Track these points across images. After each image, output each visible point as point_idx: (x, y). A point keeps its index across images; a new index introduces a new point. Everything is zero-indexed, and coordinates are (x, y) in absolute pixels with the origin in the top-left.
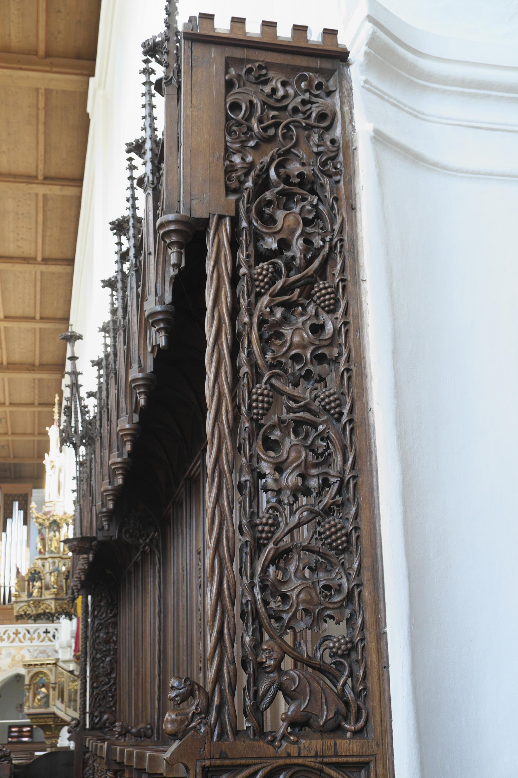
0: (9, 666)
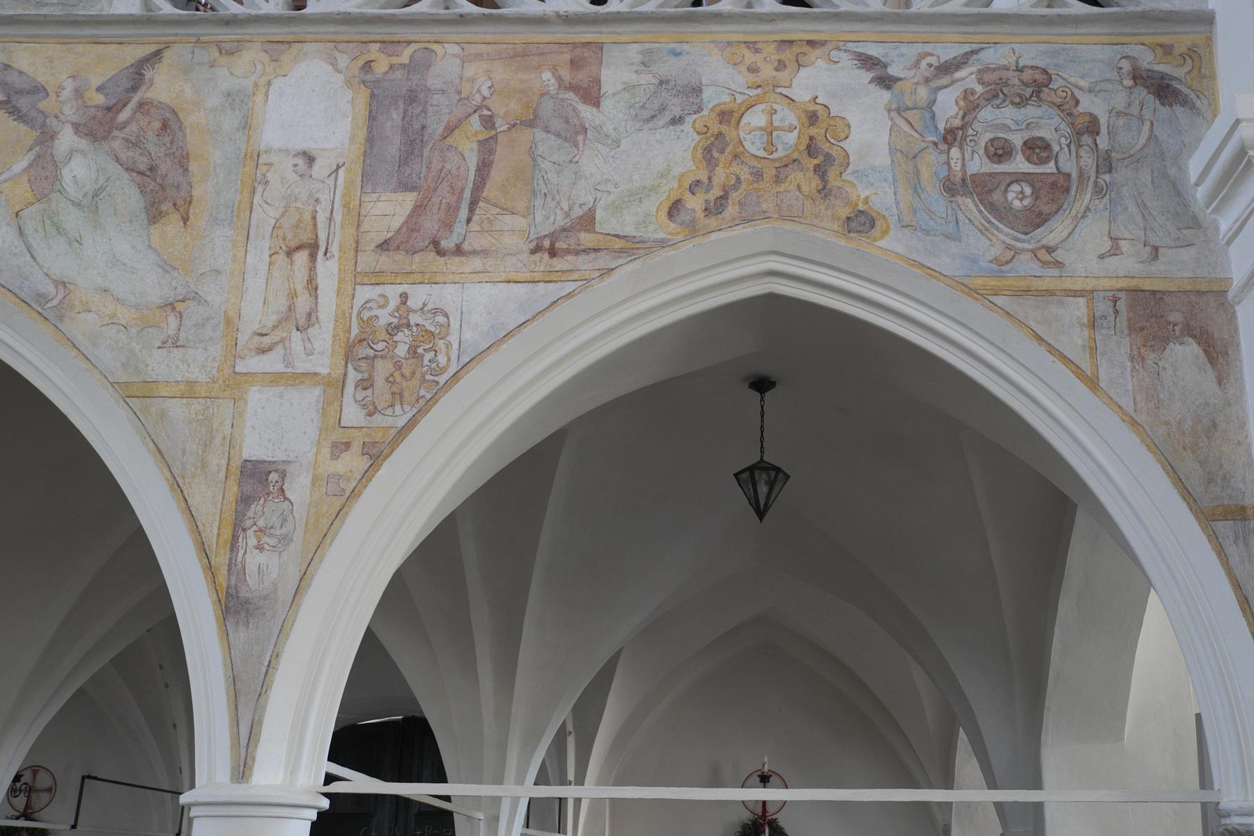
0: (675, 208)
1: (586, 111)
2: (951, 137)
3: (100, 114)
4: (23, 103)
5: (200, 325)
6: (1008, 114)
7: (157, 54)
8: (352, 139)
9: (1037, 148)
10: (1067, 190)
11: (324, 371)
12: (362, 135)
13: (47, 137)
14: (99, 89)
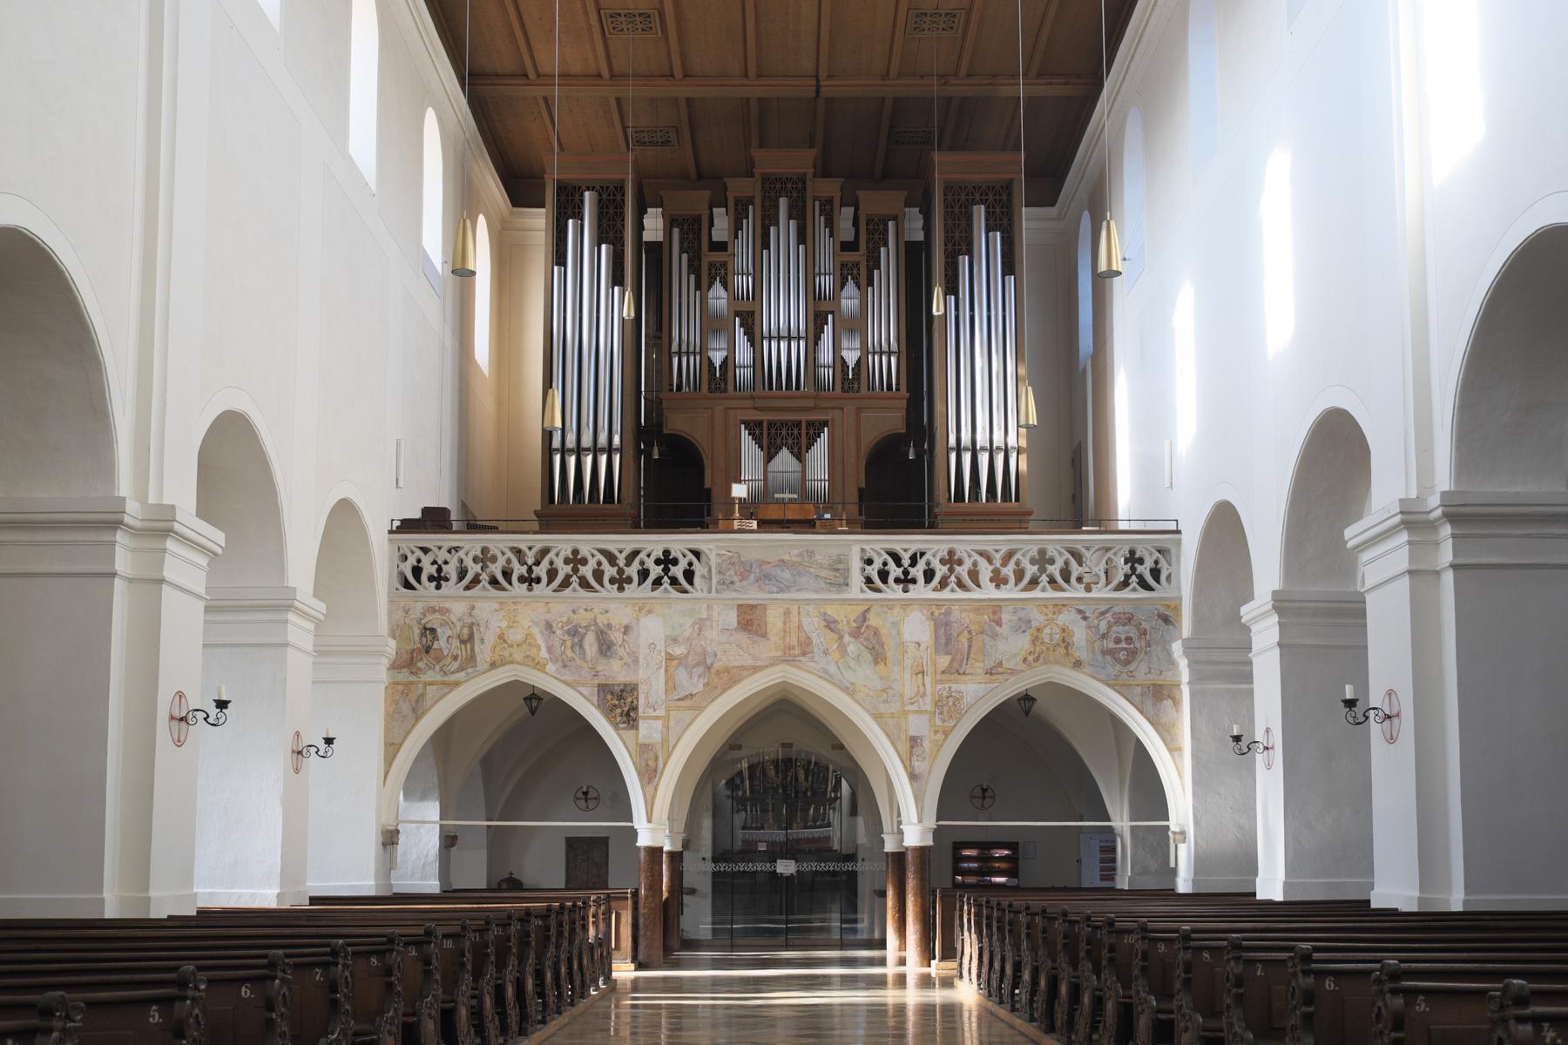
0: (1025, 660)
1: (998, 628)
2: (1104, 636)
3: (856, 630)
4: (832, 626)
5: (894, 696)
6: (1121, 628)
7: (869, 609)
8: (931, 638)
9: (1129, 640)
10: (1136, 653)
11: (929, 709)
12: (933, 637)
13: (841, 637)
14: (854, 621)
